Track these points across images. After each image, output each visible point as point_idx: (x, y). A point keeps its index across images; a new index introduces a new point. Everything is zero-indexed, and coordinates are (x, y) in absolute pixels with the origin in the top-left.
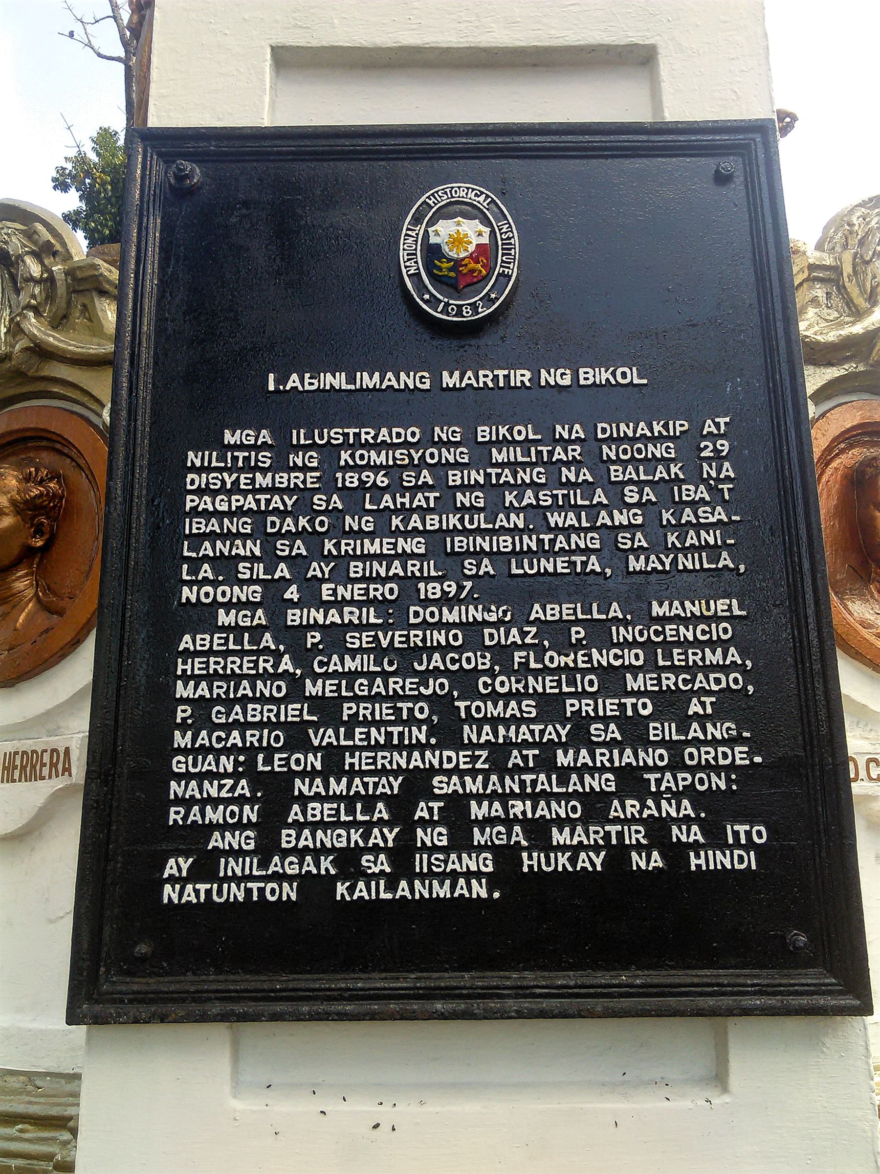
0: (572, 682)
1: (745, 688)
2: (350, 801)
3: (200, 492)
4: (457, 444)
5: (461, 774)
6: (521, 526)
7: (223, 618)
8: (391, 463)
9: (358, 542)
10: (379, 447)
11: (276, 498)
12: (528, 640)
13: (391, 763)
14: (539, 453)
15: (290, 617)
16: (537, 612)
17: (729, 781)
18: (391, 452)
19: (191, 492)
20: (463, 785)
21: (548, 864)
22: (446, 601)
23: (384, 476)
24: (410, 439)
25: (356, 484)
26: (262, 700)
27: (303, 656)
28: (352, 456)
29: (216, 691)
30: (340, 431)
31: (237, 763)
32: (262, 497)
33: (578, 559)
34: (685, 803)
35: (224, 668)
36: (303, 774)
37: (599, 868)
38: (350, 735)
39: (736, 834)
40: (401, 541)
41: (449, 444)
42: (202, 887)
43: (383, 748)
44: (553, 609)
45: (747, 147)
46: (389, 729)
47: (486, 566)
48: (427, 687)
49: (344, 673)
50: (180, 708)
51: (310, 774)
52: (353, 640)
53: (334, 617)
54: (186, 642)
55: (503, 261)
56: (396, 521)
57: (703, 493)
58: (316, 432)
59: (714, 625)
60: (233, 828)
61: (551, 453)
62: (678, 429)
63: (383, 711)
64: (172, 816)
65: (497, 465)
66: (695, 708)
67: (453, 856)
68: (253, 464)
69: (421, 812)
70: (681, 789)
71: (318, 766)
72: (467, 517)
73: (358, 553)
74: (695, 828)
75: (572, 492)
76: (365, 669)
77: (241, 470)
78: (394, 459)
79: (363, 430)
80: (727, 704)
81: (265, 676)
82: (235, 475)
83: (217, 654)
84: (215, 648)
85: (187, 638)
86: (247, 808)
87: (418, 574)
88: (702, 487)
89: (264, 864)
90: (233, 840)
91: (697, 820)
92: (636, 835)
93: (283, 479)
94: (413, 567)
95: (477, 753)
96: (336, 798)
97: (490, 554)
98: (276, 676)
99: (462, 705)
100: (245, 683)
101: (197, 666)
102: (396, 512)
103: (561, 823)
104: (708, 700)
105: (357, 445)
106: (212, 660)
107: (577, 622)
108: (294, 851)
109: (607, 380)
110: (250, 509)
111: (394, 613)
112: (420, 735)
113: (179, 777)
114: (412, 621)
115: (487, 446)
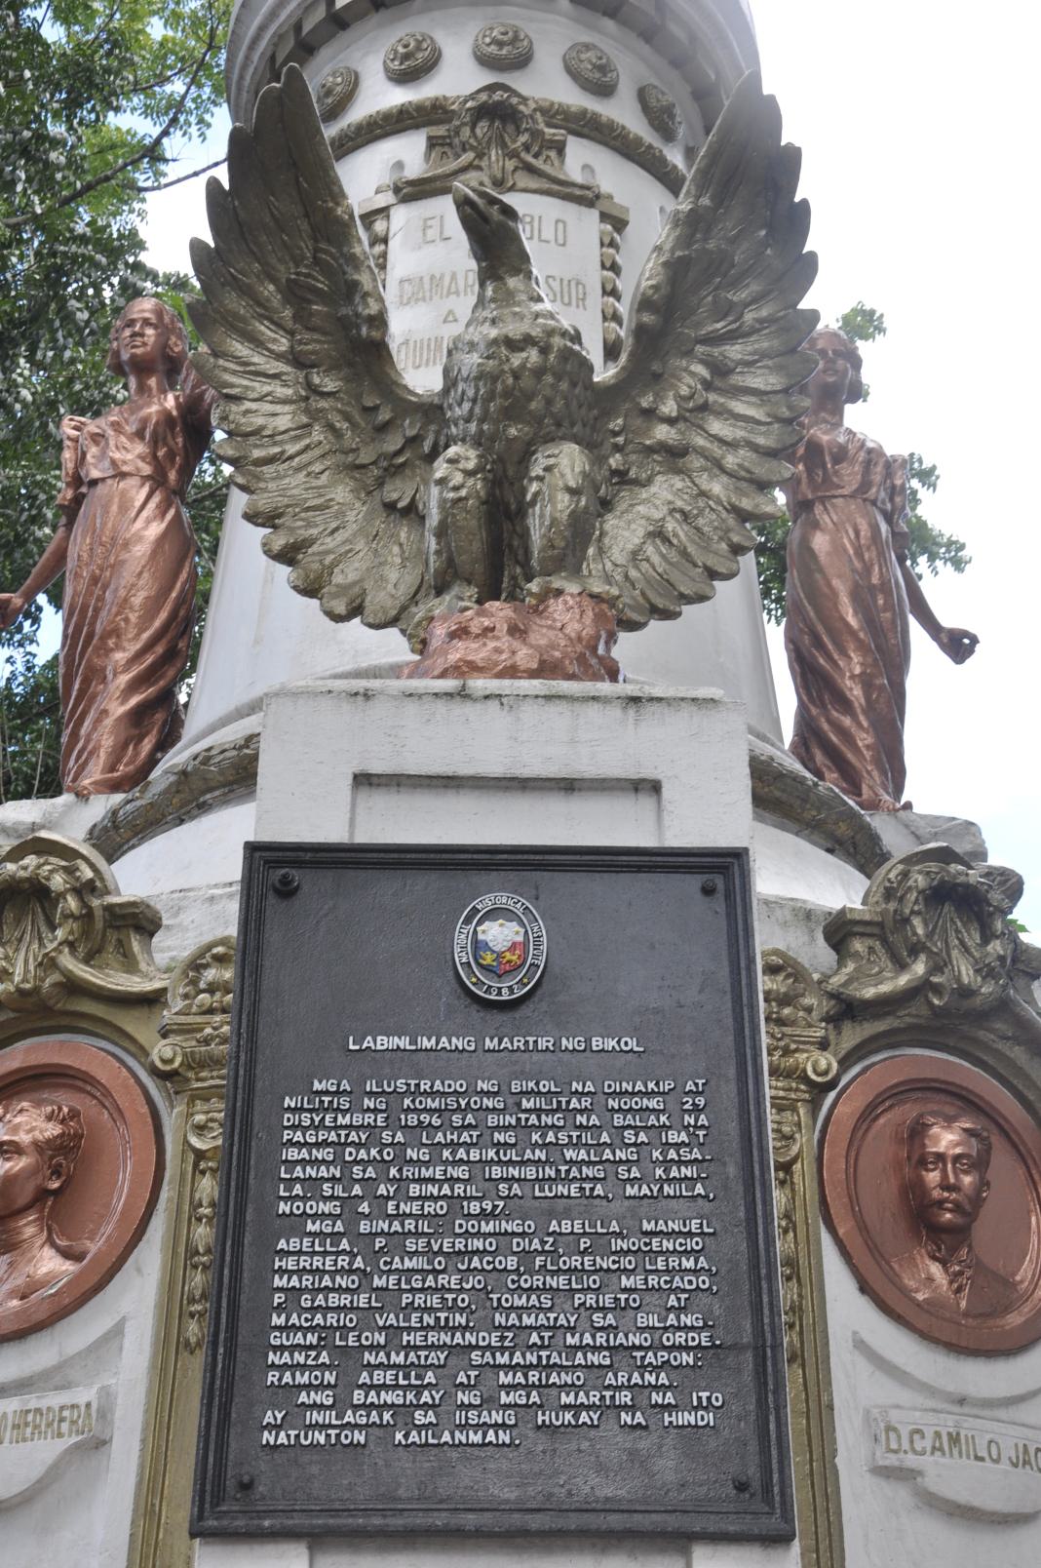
0: (579, 1281)
2: (405, 1368)
3: (294, 1127)
4: (496, 1094)
7: (310, 1227)
10: (432, 1094)
16: (554, 1226)
17: (696, 1359)
22: (483, 1215)
26: (340, 1290)
31: (320, 1338)
32: (343, 1133)
33: (587, 1186)
38: (407, 1319)
39: (699, 1398)
41: (488, 1094)
42: (293, 1433)
43: (433, 1328)
47: (516, 1189)
51: (374, 1348)
53: (396, 1226)
56: (446, 1154)
57: (683, 1137)
60: (316, 1388)
63: (435, 1301)
65: (526, 1111)
81: (342, 1271)
83: (306, 1253)
90: (317, 1397)
94: (459, 1189)
97: (519, 1180)
98: (351, 1271)
102: (446, 1145)
103: (565, 1387)
104: (683, 1296)
108: (363, 1406)
111: (441, 1225)
112: (460, 1319)
113: (275, 1349)
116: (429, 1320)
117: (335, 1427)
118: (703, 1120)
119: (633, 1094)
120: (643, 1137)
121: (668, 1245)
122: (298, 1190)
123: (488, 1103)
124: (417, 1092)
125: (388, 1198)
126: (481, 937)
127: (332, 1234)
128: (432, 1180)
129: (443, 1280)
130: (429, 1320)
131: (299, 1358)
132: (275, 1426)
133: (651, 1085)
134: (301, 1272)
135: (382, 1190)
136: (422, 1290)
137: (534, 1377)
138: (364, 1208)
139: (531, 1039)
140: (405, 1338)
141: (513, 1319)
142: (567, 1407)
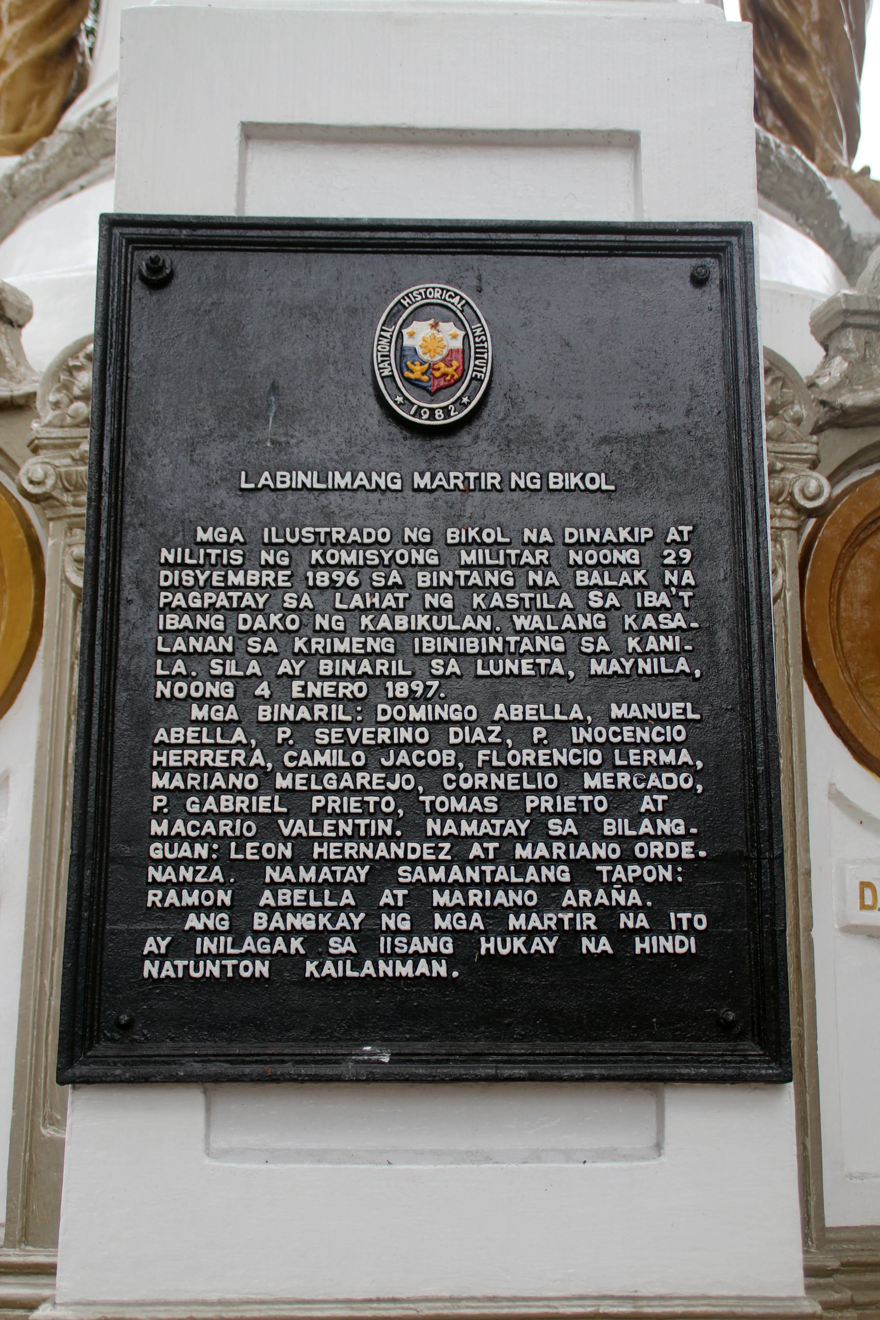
0: (532, 780)
1: (694, 788)
2: (318, 887)
3: (172, 588)
4: (428, 545)
5: (425, 864)
6: (488, 627)
7: (197, 713)
8: (361, 563)
9: (329, 641)
11: (248, 595)
12: (492, 739)
13: (358, 853)
14: (507, 556)
15: (261, 713)
16: (500, 712)
17: (675, 873)
18: (361, 552)
19: (165, 589)
21: (504, 946)
23: (355, 575)
24: (380, 539)
25: (327, 583)
26: (234, 791)
27: (274, 750)
28: (323, 555)
29: (190, 782)
30: (312, 530)
32: (235, 595)
33: (543, 661)
34: (634, 893)
35: (198, 760)
36: (274, 862)
37: (551, 951)
38: (319, 826)
39: (679, 921)
40: (370, 640)
41: (418, 544)
42: (180, 964)
43: (350, 838)
45: (723, 249)
46: (357, 821)
47: (454, 667)
48: (393, 782)
49: (313, 767)
50: (156, 798)
52: (321, 735)
53: (304, 713)
54: (161, 735)
55: (475, 366)
57: (664, 599)
58: (288, 530)
59: (668, 728)
60: (208, 910)
61: (519, 556)
62: (643, 536)
63: (353, 804)
64: (151, 898)
65: (466, 567)
66: (646, 804)
67: (416, 940)
68: (225, 561)
69: (386, 898)
71: (288, 854)
72: (435, 618)
73: (329, 650)
74: (641, 916)
75: (538, 596)
76: (334, 764)
77: (213, 567)
78: (365, 558)
79: (334, 530)
80: (677, 802)
81: (237, 769)
82: (207, 573)
84: (190, 741)
86: (221, 893)
87: (386, 673)
88: (663, 595)
89: (236, 944)
91: (644, 908)
92: (589, 921)
93: (254, 577)
94: (382, 666)
95: (440, 845)
96: (304, 885)
97: (457, 655)
98: (247, 769)
99: (428, 799)
100: (218, 775)
101: (172, 758)
102: (365, 611)
103: (517, 909)
104: (660, 798)
105: (328, 542)
106: (187, 752)
107: (540, 722)
108: (266, 932)
109: (576, 485)
110: (223, 607)
113: (156, 863)
114: (381, 718)
115: (457, 548)
117: (232, 956)
118: (688, 577)
119: (600, 545)
120: (612, 600)
122: (179, 667)
123: (418, 556)
124: (328, 543)
125: (293, 677)
126: (407, 342)
127: (223, 722)
128: (349, 656)
129: (362, 779)
131: (186, 874)
132: (160, 955)
133: (624, 534)
134: (184, 770)
135: (285, 667)
136: (337, 792)
137: (475, 896)
138: (263, 690)
139: (472, 475)
140: (317, 850)
141: (450, 827)
142: (518, 932)
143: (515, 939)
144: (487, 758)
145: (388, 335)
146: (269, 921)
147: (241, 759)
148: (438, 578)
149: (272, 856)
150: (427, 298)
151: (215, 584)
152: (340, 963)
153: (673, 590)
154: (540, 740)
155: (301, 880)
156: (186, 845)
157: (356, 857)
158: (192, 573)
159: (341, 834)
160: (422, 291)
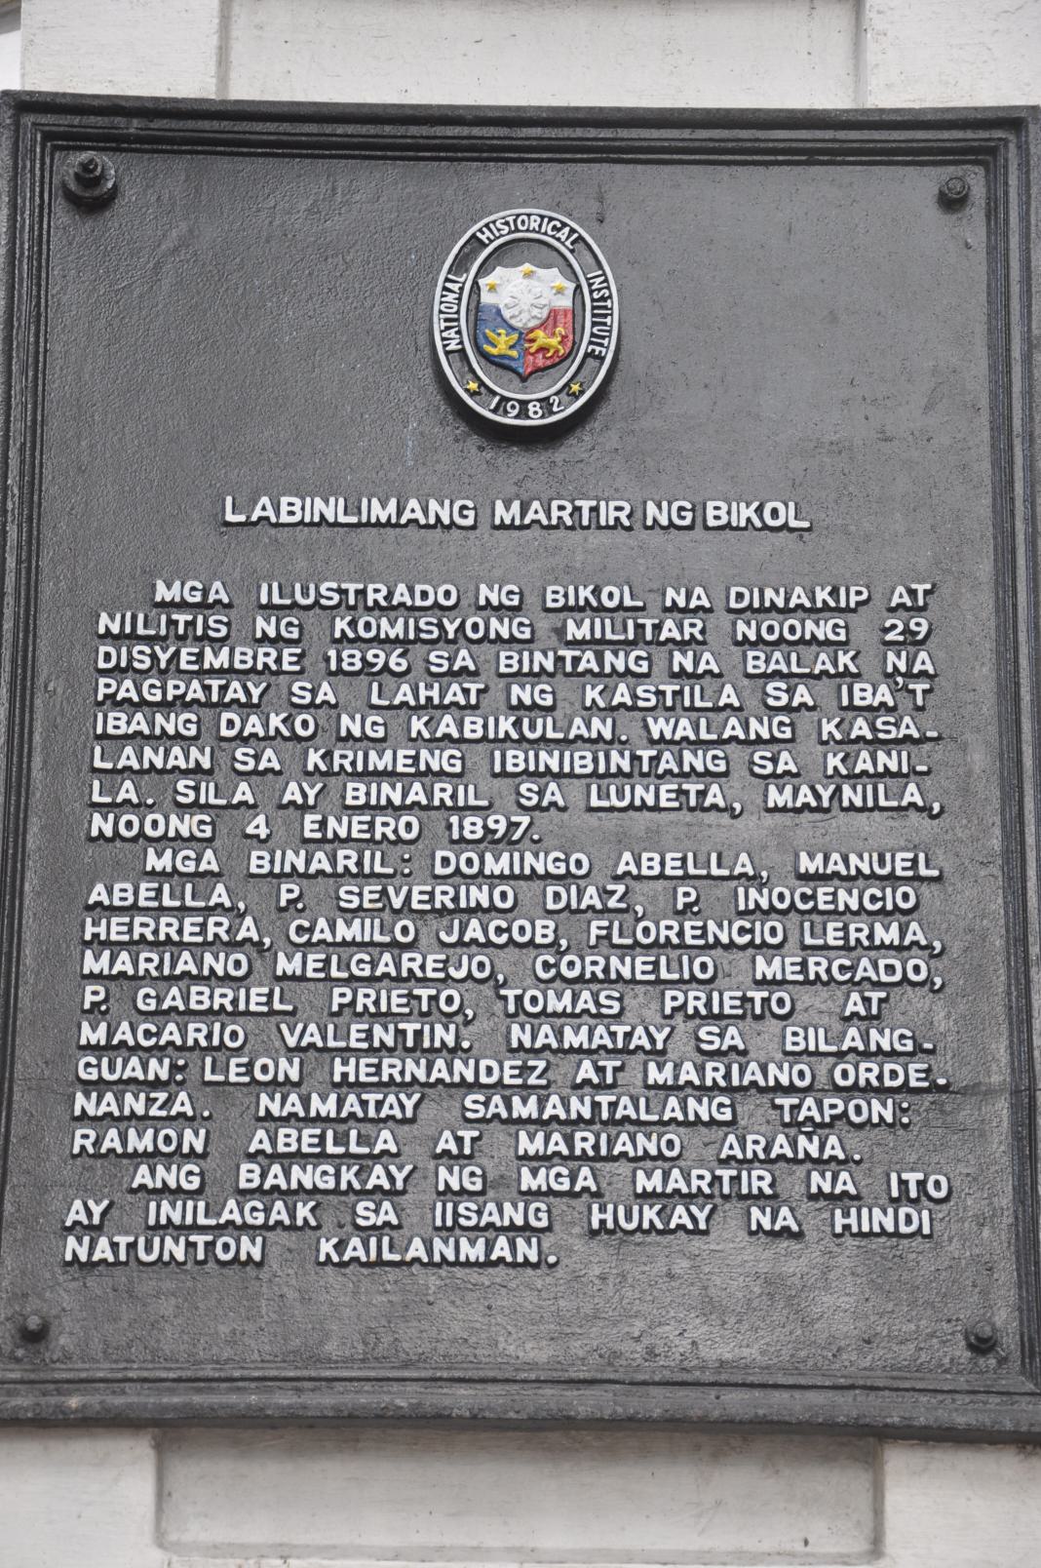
0: (675, 965)
3: (118, 672)
6: (608, 735)
7: (153, 862)
8: (412, 636)
9: (360, 754)
11: (235, 684)
12: (612, 903)
13: (402, 1073)
14: (639, 628)
15: (254, 862)
16: (626, 863)
18: (411, 622)
20: (509, 1107)
24: (442, 601)
25: (358, 666)
28: (353, 624)
29: (142, 966)
32: (215, 684)
33: (693, 788)
35: (156, 932)
38: (342, 1033)
43: (391, 1051)
44: (650, 859)
45: (993, 151)
46: (401, 1026)
47: (553, 792)
49: (334, 944)
50: (89, 989)
53: (321, 862)
55: (593, 335)
57: (884, 694)
58: (298, 587)
59: (889, 891)
61: (657, 628)
62: (854, 599)
63: (395, 1000)
64: (78, 1142)
68: (199, 632)
70: (827, 1120)
72: (526, 721)
73: (360, 768)
75: (687, 689)
76: (367, 939)
77: (182, 638)
78: (418, 629)
84: (142, 903)
85: (100, 887)
86: (188, 1134)
87: (449, 803)
94: (442, 792)
95: (531, 1063)
97: (558, 776)
98: (234, 945)
100: (186, 955)
101: (114, 929)
104: (876, 996)
105: (361, 606)
106: (138, 920)
109: (749, 520)
110: (195, 701)
112: (445, 1035)
113: (87, 1086)
114: (439, 870)
115: (562, 615)
116: (383, 1035)
117: (204, 1229)
118: (923, 662)
119: (786, 611)
120: (802, 695)
121: (847, 899)
122: (127, 791)
123: (500, 627)
124: (361, 605)
125: (304, 808)
126: (486, 298)
127: (197, 874)
128: (390, 775)
129: (410, 962)
130: (383, 1035)
132: (90, 1227)
133: (822, 595)
135: (292, 793)
136: (371, 980)
138: (258, 826)
139: (586, 505)
141: (546, 1035)
142: (647, 1196)
143: (646, 1208)
144: (604, 932)
145: (455, 287)
146: (263, 1176)
147: (221, 931)
148: (531, 661)
149: (269, 1077)
150: (517, 230)
151: (184, 666)
152: (373, 1241)
153: (900, 679)
154: (688, 906)
155: (313, 1114)
156: (134, 1061)
157: (398, 1079)
158: (148, 650)
159: (376, 1044)
160: (511, 219)
